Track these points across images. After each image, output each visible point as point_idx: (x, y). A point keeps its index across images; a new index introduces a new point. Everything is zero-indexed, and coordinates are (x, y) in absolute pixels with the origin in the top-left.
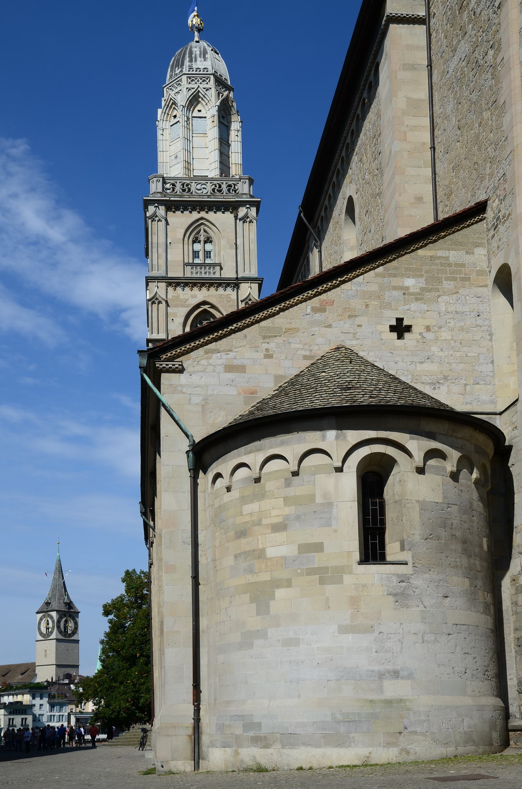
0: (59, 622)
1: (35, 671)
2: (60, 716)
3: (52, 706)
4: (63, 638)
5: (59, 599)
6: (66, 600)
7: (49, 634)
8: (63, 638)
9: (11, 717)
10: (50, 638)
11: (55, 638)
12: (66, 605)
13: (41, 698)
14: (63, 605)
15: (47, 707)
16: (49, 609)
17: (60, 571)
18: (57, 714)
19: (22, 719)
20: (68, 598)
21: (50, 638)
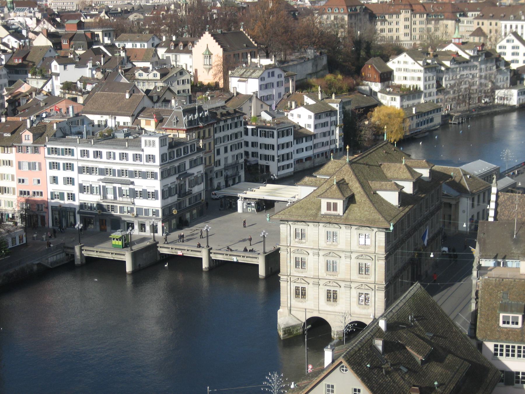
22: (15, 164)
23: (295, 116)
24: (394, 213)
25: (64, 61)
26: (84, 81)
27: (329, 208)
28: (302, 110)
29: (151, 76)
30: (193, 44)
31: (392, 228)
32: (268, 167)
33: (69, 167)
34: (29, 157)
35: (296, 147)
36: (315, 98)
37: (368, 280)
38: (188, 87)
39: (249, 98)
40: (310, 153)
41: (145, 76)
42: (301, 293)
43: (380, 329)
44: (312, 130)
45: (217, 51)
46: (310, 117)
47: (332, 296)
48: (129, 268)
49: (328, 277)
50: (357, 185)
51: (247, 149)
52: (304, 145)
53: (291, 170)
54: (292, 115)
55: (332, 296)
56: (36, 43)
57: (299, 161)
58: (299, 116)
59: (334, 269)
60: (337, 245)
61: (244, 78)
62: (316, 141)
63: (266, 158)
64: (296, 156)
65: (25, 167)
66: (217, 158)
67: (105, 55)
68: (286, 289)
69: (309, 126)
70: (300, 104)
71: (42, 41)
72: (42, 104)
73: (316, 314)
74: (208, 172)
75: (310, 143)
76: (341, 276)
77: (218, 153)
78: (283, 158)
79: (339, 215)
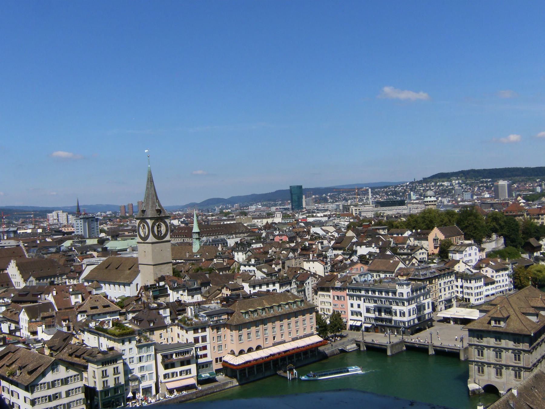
0: (153, 227)
1: (138, 267)
2: (148, 356)
3: (140, 347)
4: (157, 241)
5: (152, 207)
6: (158, 208)
7: (147, 237)
8: (157, 241)
9: (104, 369)
10: (147, 241)
11: (151, 242)
12: (158, 212)
13: (130, 342)
14: (155, 212)
15: (136, 350)
16: (145, 217)
17: (150, 180)
18: (145, 355)
19: (114, 368)
20: (160, 205)
21: (147, 241)
22: (332, 297)
23: (485, 271)
24: (534, 326)
25: (360, 244)
26: (370, 254)
27: (496, 323)
28: (487, 268)
29: (406, 251)
30: (428, 234)
31: (532, 335)
32: (469, 299)
33: (359, 297)
34: (339, 293)
35: (485, 288)
36: (496, 262)
37: (519, 365)
38: (425, 256)
39: (458, 262)
40: (493, 291)
41: (402, 251)
42: (481, 371)
43: (512, 395)
44: (495, 279)
45: (441, 237)
46: (493, 272)
47: (499, 373)
48: (389, 353)
49: (496, 362)
50: (512, 310)
51: (457, 289)
52: (490, 287)
53: (482, 301)
54: (483, 271)
55: (499, 373)
56: (347, 235)
57: (487, 296)
58: (487, 271)
59: (500, 358)
60: (501, 344)
61: (455, 251)
62: (496, 285)
63: (468, 294)
64: (485, 293)
65: (336, 298)
66: (440, 294)
67: (382, 240)
68: (473, 368)
69: (492, 276)
70: (488, 265)
71: (350, 233)
72: (348, 266)
73: (490, 383)
74: (435, 302)
75: (493, 286)
76: (503, 362)
77: (440, 292)
78: (478, 294)
79: (501, 327)
